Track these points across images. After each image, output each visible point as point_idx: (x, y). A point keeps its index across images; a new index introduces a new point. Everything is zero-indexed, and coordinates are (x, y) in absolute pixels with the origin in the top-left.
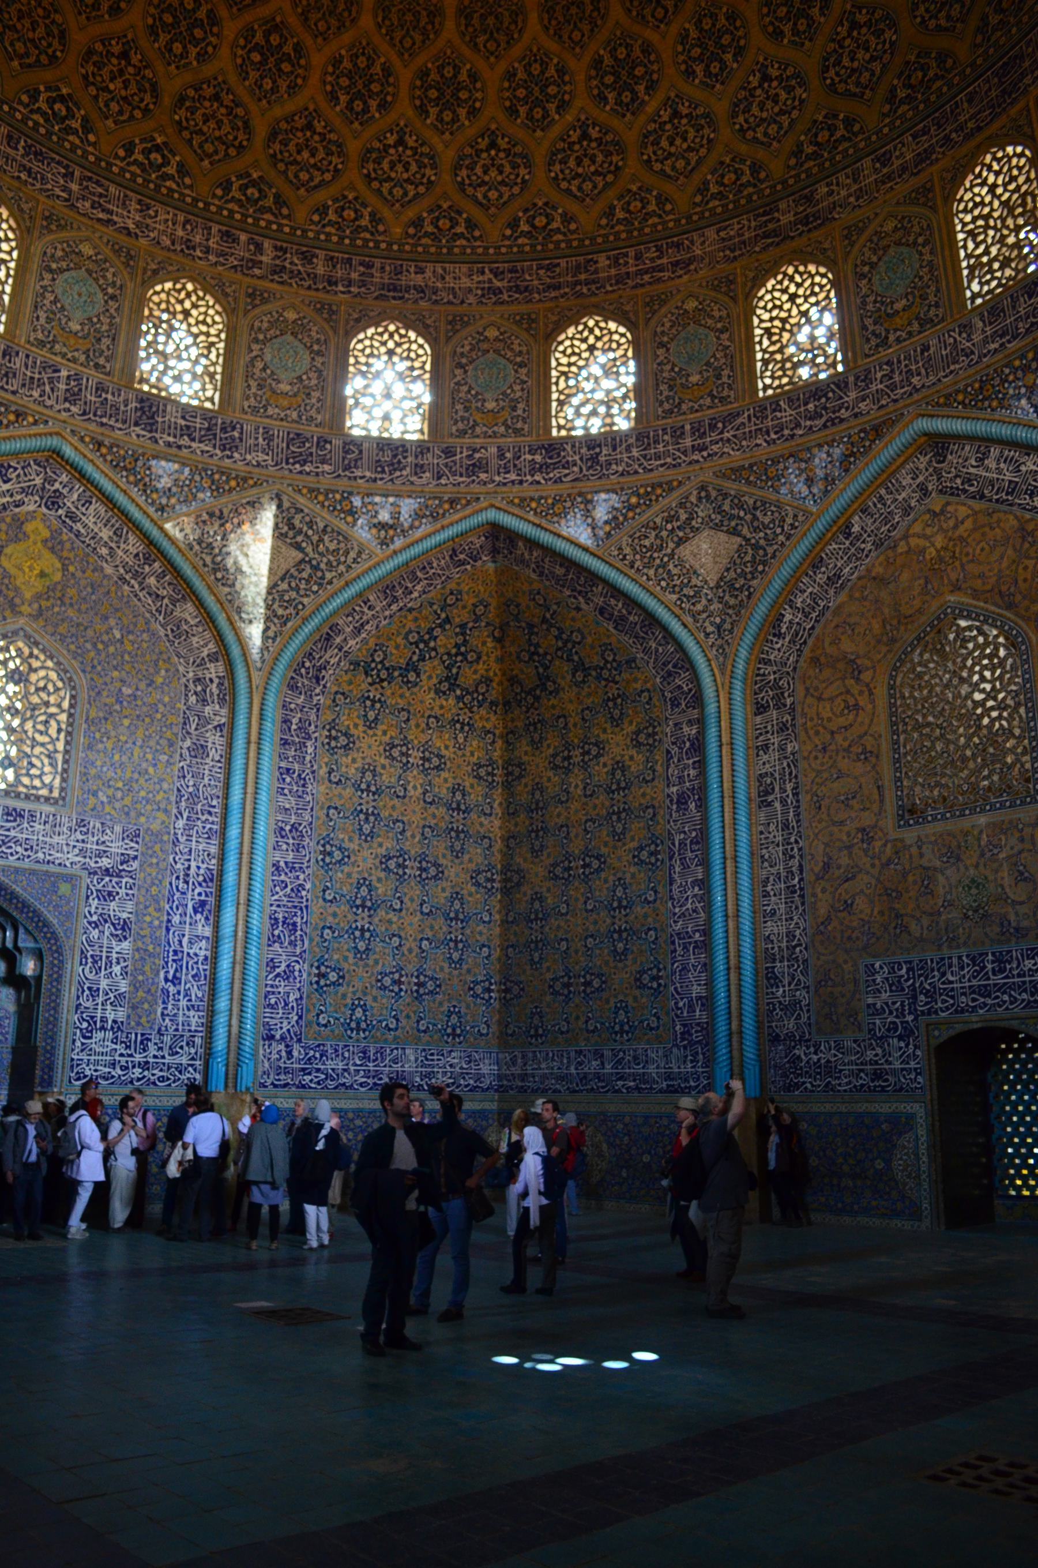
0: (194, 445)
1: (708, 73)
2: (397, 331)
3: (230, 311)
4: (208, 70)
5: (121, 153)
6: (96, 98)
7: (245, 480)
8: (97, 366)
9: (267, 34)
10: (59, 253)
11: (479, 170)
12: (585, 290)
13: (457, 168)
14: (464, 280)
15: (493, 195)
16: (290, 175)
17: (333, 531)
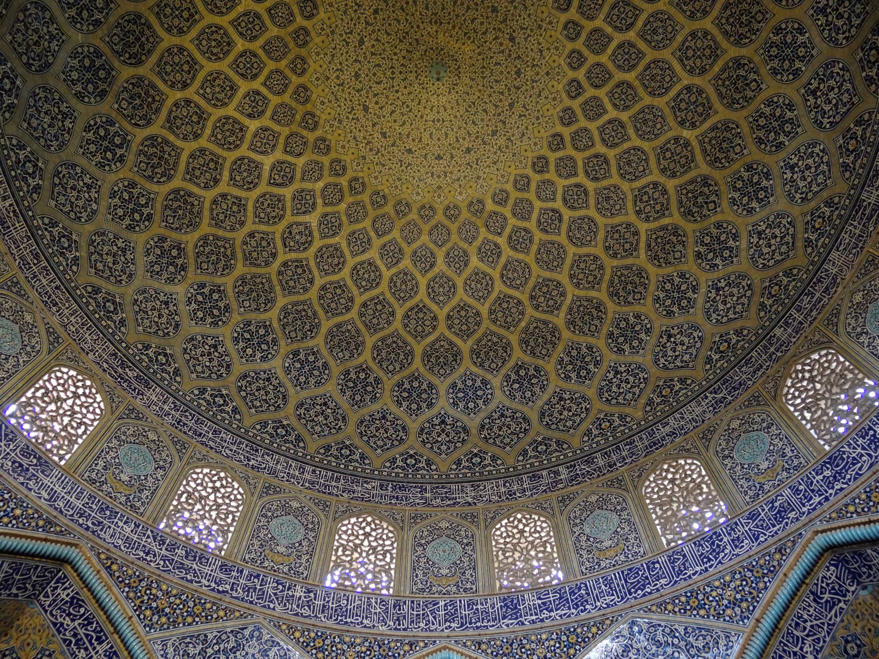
0: (552, 614)
1: (760, 201)
2: (670, 466)
3: (551, 516)
4: (492, 406)
5: (454, 467)
6: (432, 448)
7: (602, 623)
8: (465, 590)
9: (517, 373)
10: (426, 533)
11: (670, 353)
12: (779, 354)
13: (656, 362)
14: (696, 409)
15: (686, 357)
16: (561, 428)
17: (694, 630)
